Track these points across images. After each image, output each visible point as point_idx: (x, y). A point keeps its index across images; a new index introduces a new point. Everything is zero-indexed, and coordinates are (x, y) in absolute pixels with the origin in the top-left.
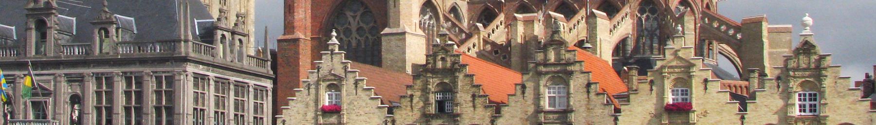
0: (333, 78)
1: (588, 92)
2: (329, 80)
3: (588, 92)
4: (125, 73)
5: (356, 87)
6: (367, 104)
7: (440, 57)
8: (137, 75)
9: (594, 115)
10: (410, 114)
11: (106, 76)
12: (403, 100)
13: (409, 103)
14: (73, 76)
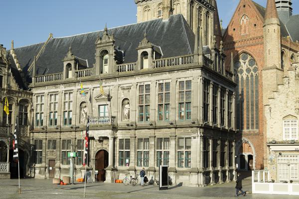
14: (125, 85)
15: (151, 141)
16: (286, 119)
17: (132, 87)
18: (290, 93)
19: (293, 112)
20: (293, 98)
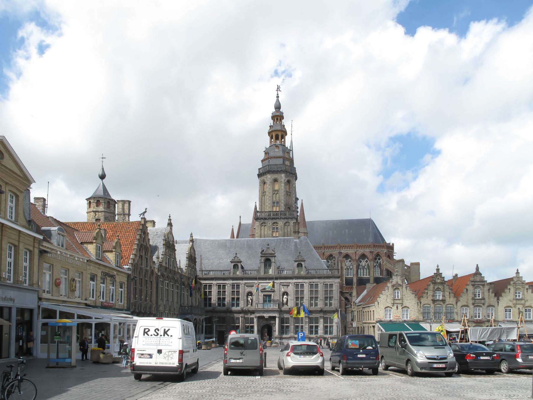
0: (397, 285)
1: (489, 292)
2: (396, 286)
3: (489, 292)
4: (310, 282)
5: (406, 289)
6: (410, 296)
7: (438, 278)
8: (316, 283)
9: (491, 300)
10: (426, 299)
11: (301, 283)
12: (424, 294)
13: (426, 296)
15: (307, 319)
16: (386, 309)
17: (290, 285)
18: (389, 295)
19: (390, 305)
20: (390, 297)
